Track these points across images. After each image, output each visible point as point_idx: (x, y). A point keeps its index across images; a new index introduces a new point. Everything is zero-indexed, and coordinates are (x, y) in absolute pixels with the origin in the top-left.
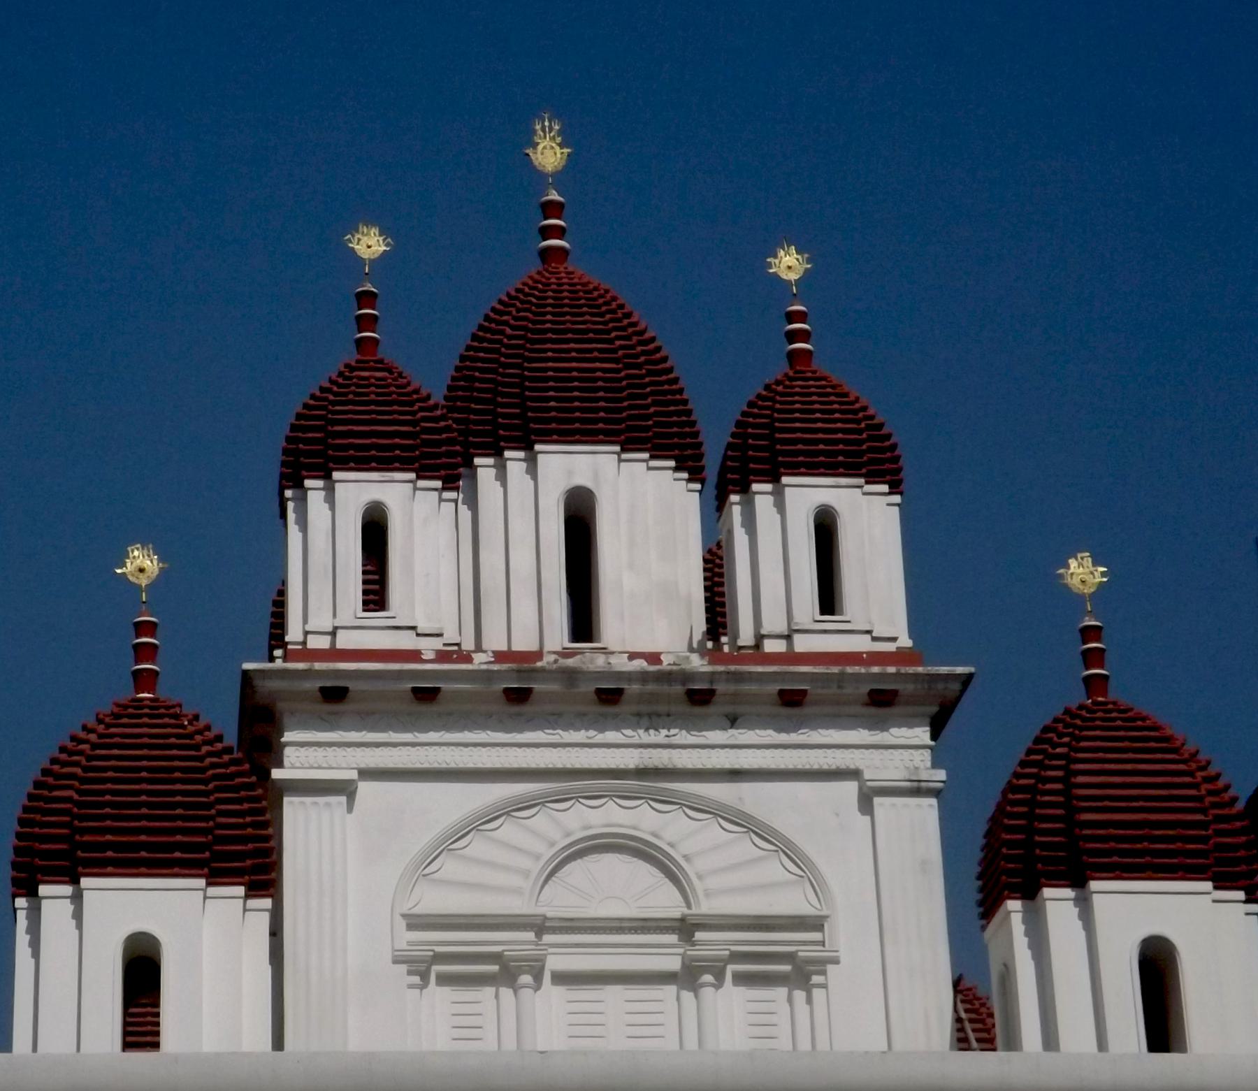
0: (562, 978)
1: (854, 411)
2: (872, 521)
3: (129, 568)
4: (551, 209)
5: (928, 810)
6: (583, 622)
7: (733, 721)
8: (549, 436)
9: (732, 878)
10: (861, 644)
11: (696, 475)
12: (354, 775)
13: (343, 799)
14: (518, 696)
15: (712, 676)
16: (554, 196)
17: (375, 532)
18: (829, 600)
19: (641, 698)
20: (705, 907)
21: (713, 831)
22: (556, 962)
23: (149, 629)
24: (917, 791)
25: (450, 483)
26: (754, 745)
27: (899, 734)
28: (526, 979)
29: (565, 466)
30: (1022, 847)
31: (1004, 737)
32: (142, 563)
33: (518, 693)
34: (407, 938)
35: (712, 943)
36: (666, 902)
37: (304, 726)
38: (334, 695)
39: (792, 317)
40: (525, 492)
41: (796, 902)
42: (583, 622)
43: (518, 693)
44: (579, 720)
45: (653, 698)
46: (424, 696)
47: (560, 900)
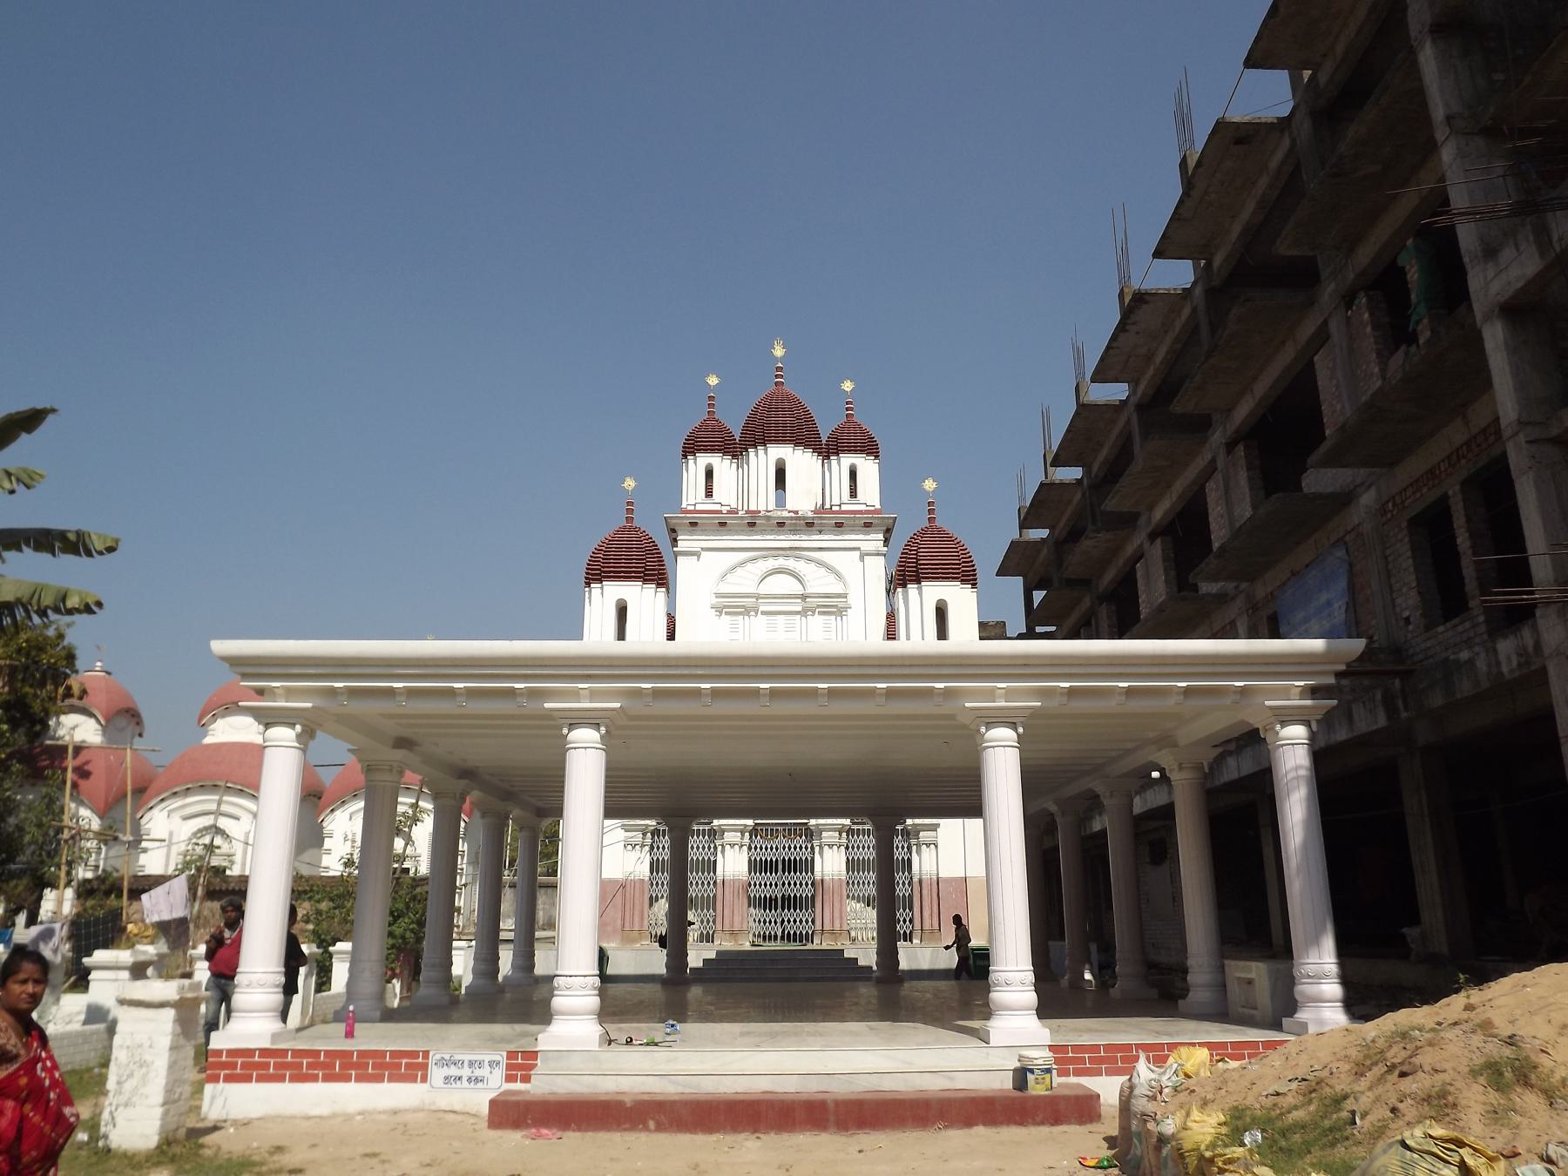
1: (864, 432)
2: (868, 469)
4: (779, 369)
6: (781, 502)
8: (771, 442)
9: (818, 581)
10: (863, 508)
11: (820, 454)
14: (752, 525)
17: (709, 474)
18: (853, 494)
20: (810, 590)
22: (762, 608)
25: (734, 456)
29: (776, 452)
30: (906, 574)
31: (901, 538)
32: (630, 484)
33: (753, 523)
34: (715, 600)
38: (693, 524)
40: (763, 460)
41: (838, 589)
42: (781, 502)
43: (753, 523)
44: (772, 532)
46: (722, 524)
47: (764, 589)
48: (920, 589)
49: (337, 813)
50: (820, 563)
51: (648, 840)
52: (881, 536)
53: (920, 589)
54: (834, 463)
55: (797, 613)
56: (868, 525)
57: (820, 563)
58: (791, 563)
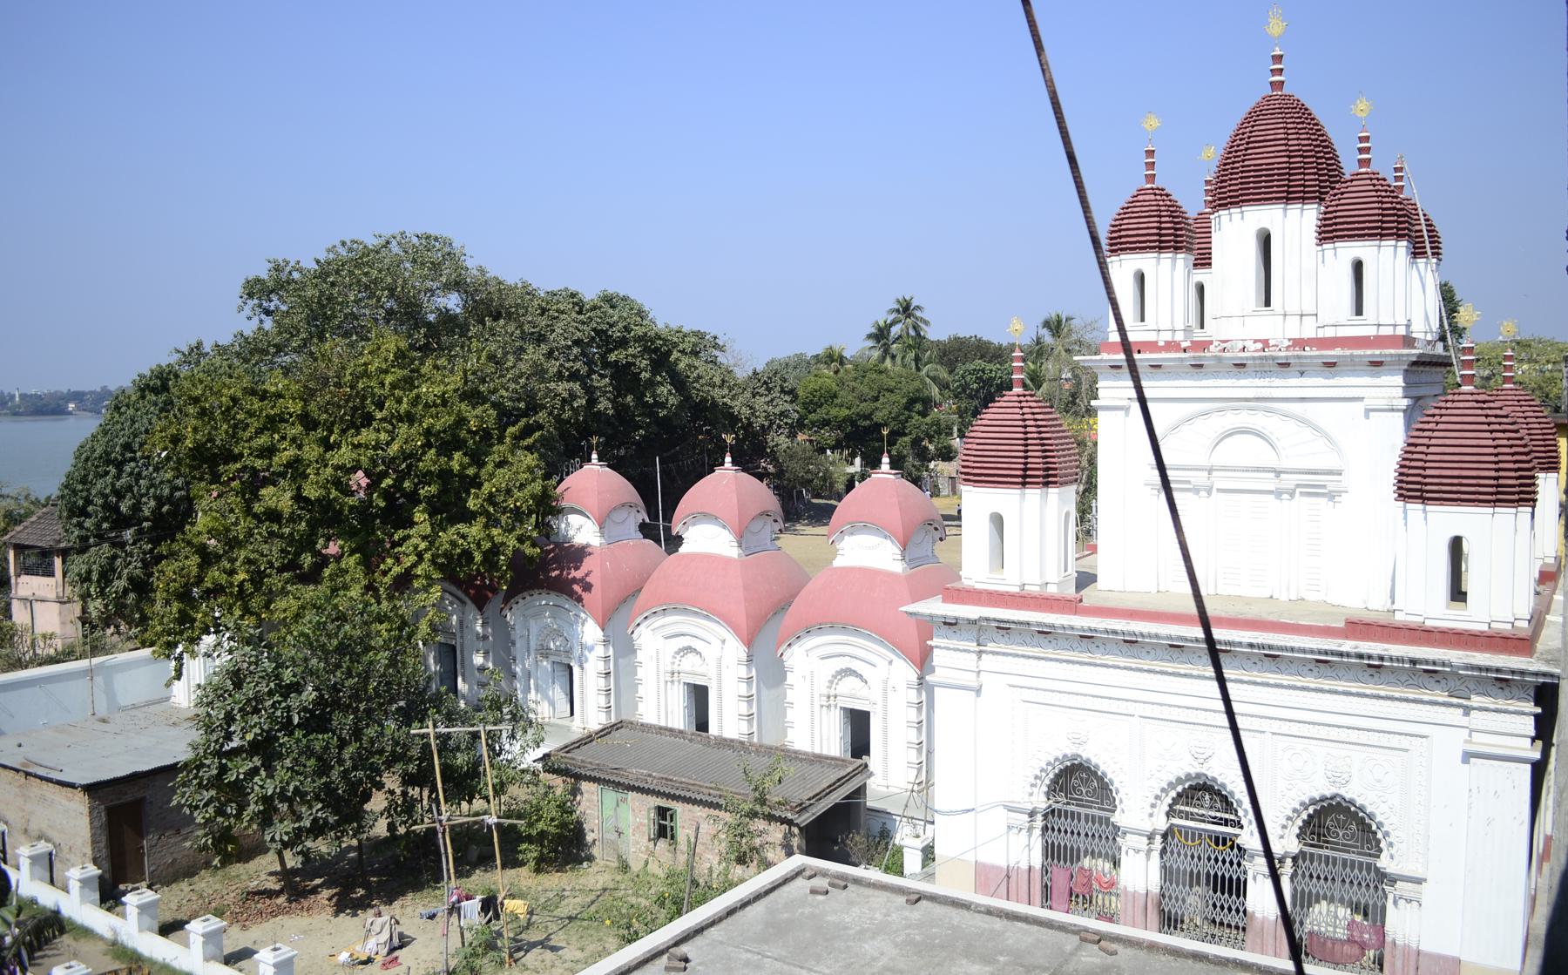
3: (1012, 328)
5: (1399, 419)
7: (1302, 374)
10: (1371, 331)
22: (1218, 485)
26: (1314, 385)
28: (1203, 494)
35: (1289, 481)
36: (1268, 458)
37: (1106, 379)
39: (1362, 139)
44: (1228, 375)
45: (1262, 365)
47: (1219, 458)
48: (1424, 511)
49: (795, 648)
50: (1303, 421)
51: (1039, 822)
52: (1399, 380)
54: (1329, 254)
57: (1303, 421)
58: (1258, 420)
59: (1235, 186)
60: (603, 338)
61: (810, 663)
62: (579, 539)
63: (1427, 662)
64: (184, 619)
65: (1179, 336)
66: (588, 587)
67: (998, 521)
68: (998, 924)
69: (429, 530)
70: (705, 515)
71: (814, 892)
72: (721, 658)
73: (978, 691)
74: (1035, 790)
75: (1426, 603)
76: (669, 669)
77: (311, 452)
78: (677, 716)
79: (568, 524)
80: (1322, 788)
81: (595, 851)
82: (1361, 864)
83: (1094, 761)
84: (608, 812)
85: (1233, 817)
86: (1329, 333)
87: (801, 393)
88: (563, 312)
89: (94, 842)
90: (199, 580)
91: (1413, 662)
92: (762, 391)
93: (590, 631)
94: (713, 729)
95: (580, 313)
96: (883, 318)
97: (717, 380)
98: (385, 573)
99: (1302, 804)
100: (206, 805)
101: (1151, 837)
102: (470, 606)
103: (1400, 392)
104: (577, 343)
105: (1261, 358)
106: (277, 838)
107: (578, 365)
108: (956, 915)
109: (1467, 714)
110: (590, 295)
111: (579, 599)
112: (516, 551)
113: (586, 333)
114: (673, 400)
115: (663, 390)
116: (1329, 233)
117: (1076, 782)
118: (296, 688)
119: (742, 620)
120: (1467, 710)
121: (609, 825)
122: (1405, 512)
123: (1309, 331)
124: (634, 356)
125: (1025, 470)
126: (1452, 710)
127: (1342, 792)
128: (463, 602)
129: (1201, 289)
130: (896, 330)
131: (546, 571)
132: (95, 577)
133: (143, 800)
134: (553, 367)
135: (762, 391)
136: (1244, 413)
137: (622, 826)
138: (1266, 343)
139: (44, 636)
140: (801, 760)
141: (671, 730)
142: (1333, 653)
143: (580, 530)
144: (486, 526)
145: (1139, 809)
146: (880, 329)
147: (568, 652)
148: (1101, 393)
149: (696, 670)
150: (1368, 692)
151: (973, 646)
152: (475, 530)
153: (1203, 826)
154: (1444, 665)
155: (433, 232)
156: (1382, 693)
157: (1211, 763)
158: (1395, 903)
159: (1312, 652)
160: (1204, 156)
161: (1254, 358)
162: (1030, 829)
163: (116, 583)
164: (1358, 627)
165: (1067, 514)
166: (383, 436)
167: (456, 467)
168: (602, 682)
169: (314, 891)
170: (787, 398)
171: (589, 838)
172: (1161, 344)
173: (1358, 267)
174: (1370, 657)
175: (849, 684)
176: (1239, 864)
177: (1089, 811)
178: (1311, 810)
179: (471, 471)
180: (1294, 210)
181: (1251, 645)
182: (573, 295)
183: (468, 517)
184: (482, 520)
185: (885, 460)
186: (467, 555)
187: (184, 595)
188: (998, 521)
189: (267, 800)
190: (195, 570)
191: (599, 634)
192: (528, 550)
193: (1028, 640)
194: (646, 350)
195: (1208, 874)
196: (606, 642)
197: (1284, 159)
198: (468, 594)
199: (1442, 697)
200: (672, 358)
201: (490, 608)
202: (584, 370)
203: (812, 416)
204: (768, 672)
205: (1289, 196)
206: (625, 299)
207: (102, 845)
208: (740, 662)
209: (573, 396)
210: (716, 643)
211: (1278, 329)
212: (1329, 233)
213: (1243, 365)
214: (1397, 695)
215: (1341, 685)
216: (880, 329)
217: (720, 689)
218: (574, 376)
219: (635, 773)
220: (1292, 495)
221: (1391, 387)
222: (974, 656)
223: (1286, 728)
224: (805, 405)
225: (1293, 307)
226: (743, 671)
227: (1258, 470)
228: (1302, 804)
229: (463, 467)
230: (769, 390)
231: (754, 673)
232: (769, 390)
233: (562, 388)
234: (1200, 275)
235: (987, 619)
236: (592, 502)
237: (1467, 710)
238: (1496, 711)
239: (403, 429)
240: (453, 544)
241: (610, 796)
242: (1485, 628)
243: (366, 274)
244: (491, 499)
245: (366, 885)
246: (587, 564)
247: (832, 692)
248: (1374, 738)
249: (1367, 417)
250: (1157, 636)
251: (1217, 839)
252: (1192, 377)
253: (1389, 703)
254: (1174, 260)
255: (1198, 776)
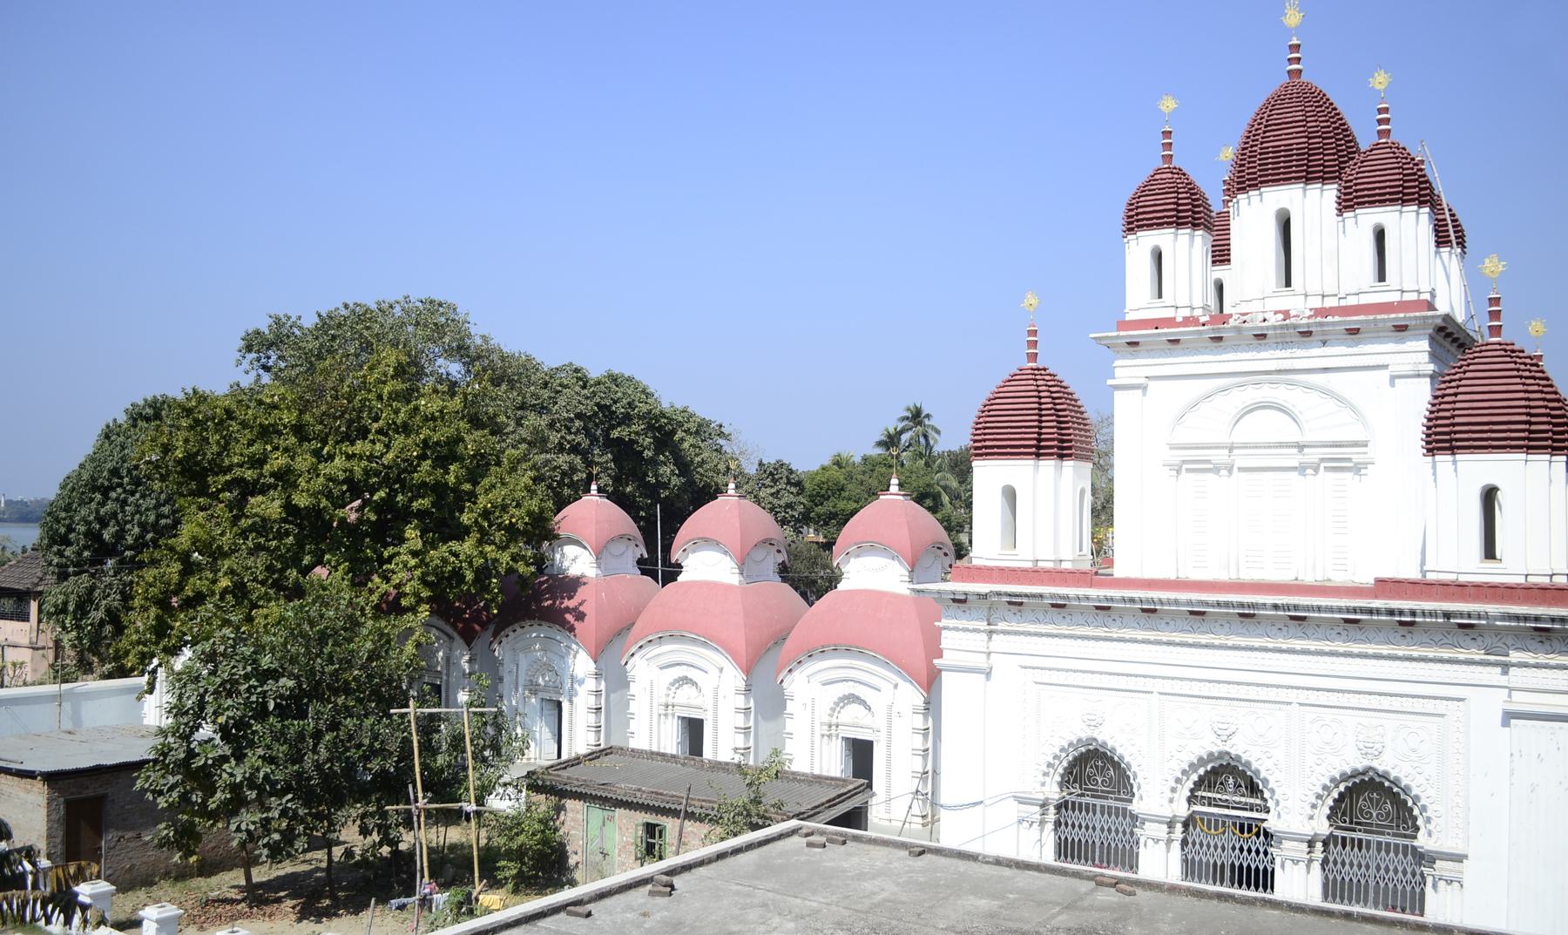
0: (1240, 469)
3: (1026, 303)
4: (1296, 48)
7: (1324, 343)
10: (1395, 297)
12: (1143, 381)
13: (1140, 392)
15: (1308, 325)
16: (1295, 41)
19: (1276, 336)
21: (1315, 397)
23: (1034, 333)
24: (1419, 376)
26: (1337, 354)
27: (1411, 345)
28: (1224, 472)
32: (1031, 299)
35: (1313, 455)
39: (1380, 111)
44: (1249, 347)
48: (1455, 462)
49: (795, 673)
50: (1327, 392)
51: (1051, 815)
52: (1424, 345)
53: (1455, 462)
54: (1350, 222)
55: (1294, 469)
56: (1401, 328)
57: (1327, 392)
58: (1279, 393)
59: (1252, 173)
60: (606, 415)
61: (811, 690)
62: (574, 571)
63: (1461, 615)
64: (161, 630)
65: (1198, 313)
66: (581, 616)
67: (1010, 495)
68: (1007, 872)
69: (420, 545)
70: (706, 540)
71: (810, 845)
72: (718, 690)
73: (988, 674)
74: (1048, 780)
75: (1458, 557)
76: (663, 701)
77: (303, 462)
78: (670, 740)
79: (563, 555)
80: (1353, 761)
81: (578, 875)
82: (1396, 846)
83: (1110, 744)
84: (594, 831)
85: (1258, 802)
86: (1352, 301)
87: (807, 485)
88: (566, 387)
89: (49, 836)
90: (180, 587)
91: (1447, 615)
92: (768, 482)
93: (581, 664)
94: (708, 753)
95: (584, 387)
96: (893, 425)
97: (722, 467)
98: (371, 592)
99: (1333, 780)
100: (171, 789)
101: (1171, 825)
102: (459, 641)
103: (1426, 357)
104: (579, 416)
105: (1282, 327)
106: (243, 827)
107: (579, 438)
108: (962, 865)
109: (1505, 673)
110: (595, 372)
111: (572, 629)
112: (510, 571)
113: (588, 408)
114: (675, 481)
115: (666, 470)
116: (1347, 203)
117: (1093, 771)
118: (273, 674)
119: (741, 646)
120: (1506, 667)
121: (594, 847)
122: (1434, 467)
123: (1331, 303)
124: (637, 433)
125: (1039, 440)
126: (1489, 669)
127: (1375, 764)
128: (451, 638)
129: (1220, 288)
130: (905, 437)
131: (536, 600)
132: (71, 608)
133: (104, 796)
134: (554, 438)
135: (768, 482)
136: (1266, 387)
137: (608, 847)
138: (1286, 314)
139: (14, 665)
140: (799, 781)
141: (663, 755)
142: (1362, 611)
143: (576, 561)
144: (480, 542)
145: (1159, 794)
146: (889, 436)
147: (558, 688)
148: (1118, 372)
149: (690, 702)
150: (1400, 653)
151: (983, 625)
152: (467, 547)
153: (1226, 812)
154: (1479, 617)
155: (438, 298)
156: (1416, 654)
157: (1234, 740)
158: (1435, 886)
159: (1340, 610)
160: (1222, 157)
161: (1275, 328)
162: (1042, 823)
163: (93, 614)
164: (1385, 586)
165: (1082, 492)
166: (379, 447)
167: (451, 479)
168: (592, 718)
169: (279, 900)
170: (793, 490)
171: (572, 861)
172: (1179, 319)
173: (1380, 235)
174: (1401, 613)
175: (852, 712)
176: (1266, 853)
177: (1105, 803)
178: (1342, 788)
179: (467, 487)
180: (1314, 189)
181: (1276, 607)
182: (577, 370)
183: (461, 533)
184: (475, 536)
185: (894, 481)
186: (457, 575)
187: (163, 603)
188: (1010, 495)
189: (235, 788)
190: (176, 578)
191: (592, 666)
192: (521, 568)
193: (1041, 617)
194: (651, 427)
195: (1233, 865)
196: (598, 676)
197: (1305, 142)
198: (454, 626)
199: (1479, 655)
200: (676, 438)
201: (478, 644)
202: (585, 443)
203: (819, 509)
204: (767, 702)
205: (1309, 175)
206: (629, 379)
207: (58, 840)
208: (738, 692)
209: (573, 469)
210: (714, 672)
211: (1299, 305)
212: (1347, 203)
213: (1264, 336)
214: (1431, 655)
215: (1371, 649)
216: (889, 436)
217: (715, 722)
218: (575, 449)
219: (623, 789)
220: (1316, 470)
221: (1417, 353)
222: (984, 636)
223: (1313, 697)
224: (812, 498)
225: (1314, 287)
226: (741, 701)
227: (1281, 445)
228: (1333, 780)
229: (459, 481)
230: (775, 481)
231: (752, 704)
232: (775, 481)
233: (563, 460)
234: (1220, 272)
235: (999, 594)
236: (589, 532)
237: (1506, 667)
238: (1537, 666)
239: (399, 441)
240: (444, 561)
241: (597, 814)
242: (1521, 580)
243: (368, 328)
244: (486, 514)
245: (333, 897)
246: (581, 594)
247: (834, 721)
248: (1408, 704)
249: (1392, 384)
250: (1176, 602)
251: (1242, 826)
252: (1211, 352)
253: (1422, 664)
254: (1192, 237)
255: (1222, 754)
